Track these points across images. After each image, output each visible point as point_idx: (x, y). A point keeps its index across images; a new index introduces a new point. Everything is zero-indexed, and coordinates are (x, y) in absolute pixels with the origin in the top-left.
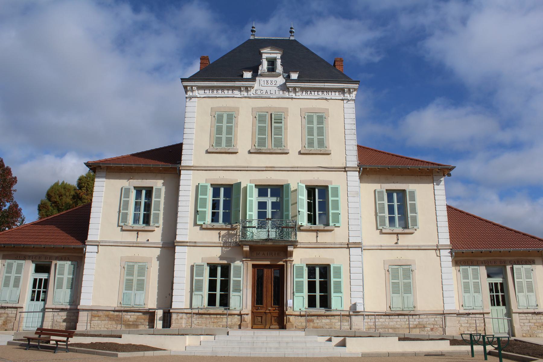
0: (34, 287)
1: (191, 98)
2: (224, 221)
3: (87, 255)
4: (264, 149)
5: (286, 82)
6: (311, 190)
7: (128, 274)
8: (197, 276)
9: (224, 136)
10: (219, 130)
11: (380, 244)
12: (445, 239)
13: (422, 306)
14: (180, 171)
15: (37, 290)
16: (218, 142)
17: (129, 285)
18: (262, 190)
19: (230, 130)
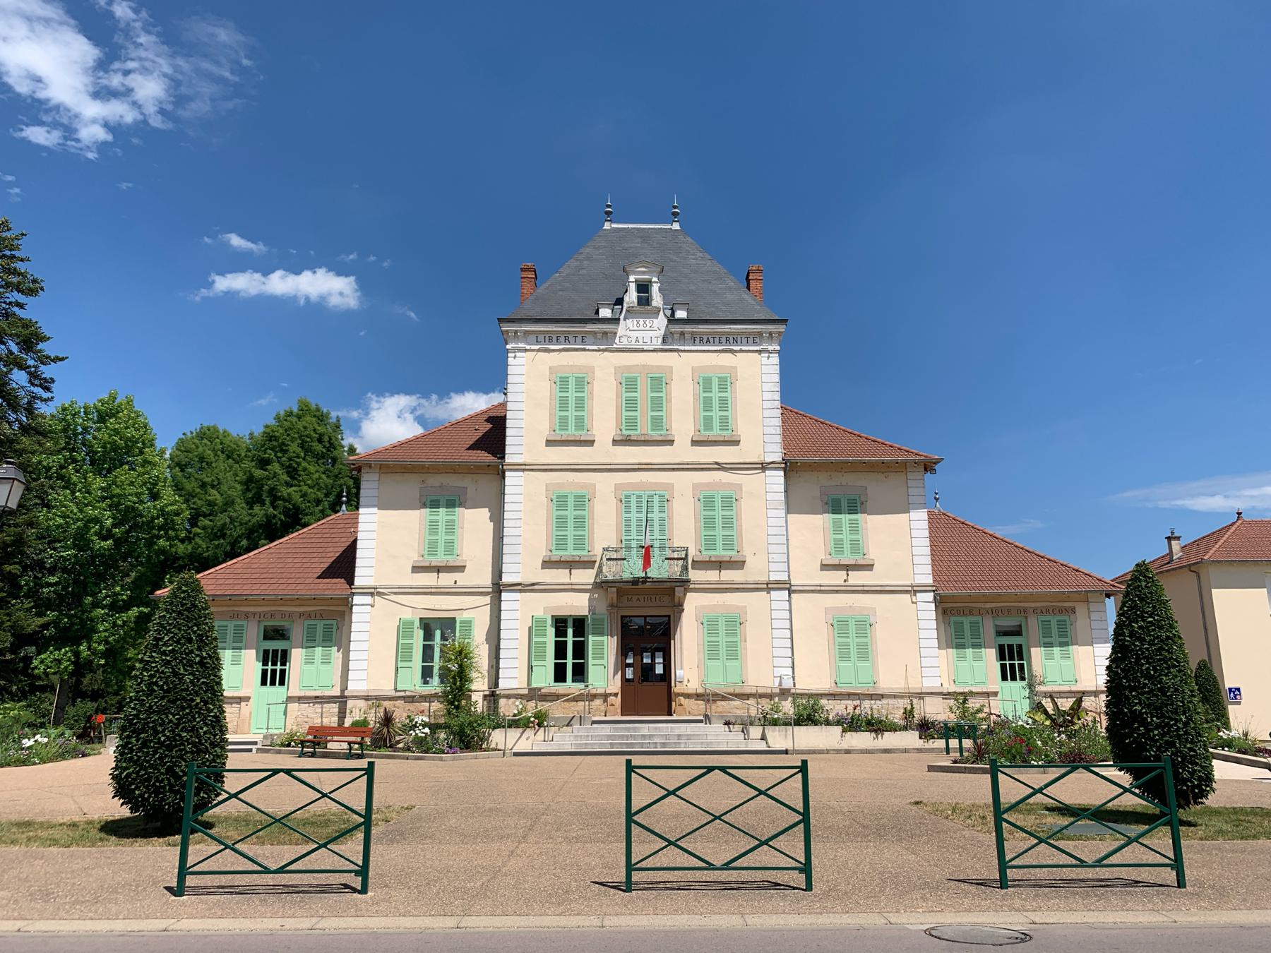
3: (355, 609)
4: (634, 434)
11: (817, 582)
13: (888, 683)
14: (504, 472)
15: (270, 667)
19: (580, 404)
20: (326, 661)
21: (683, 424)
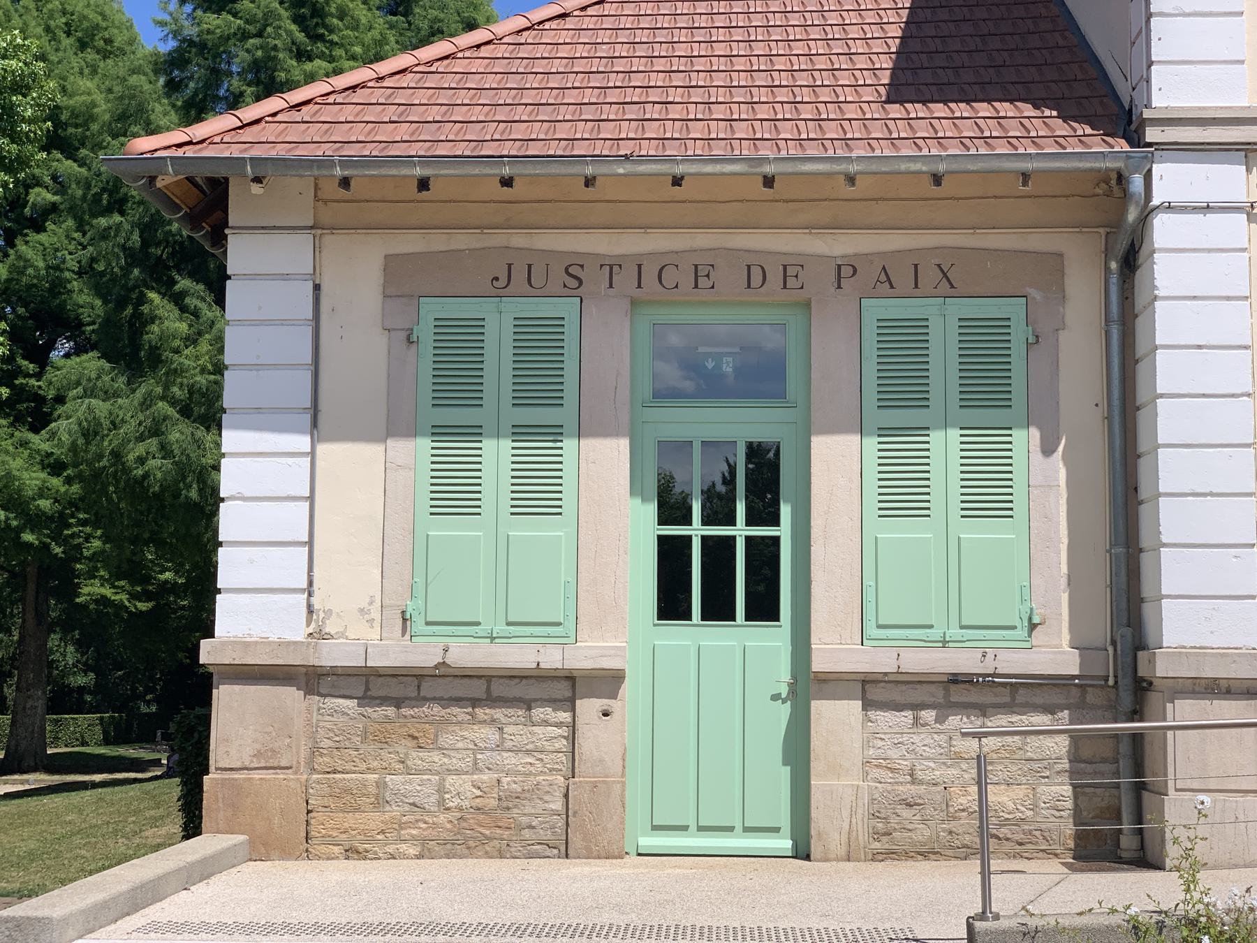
20: (988, 498)
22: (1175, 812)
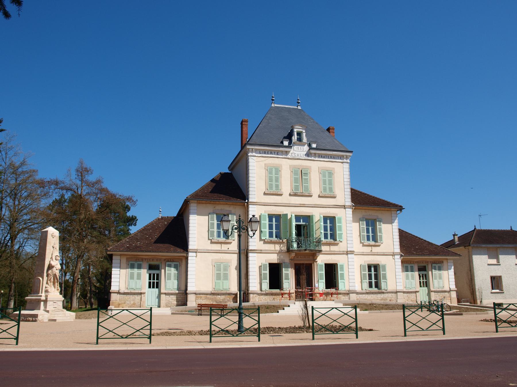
0: (150, 279)
1: (251, 156)
2: (276, 237)
5: (309, 149)
6: (325, 219)
7: (217, 270)
8: (264, 270)
9: (274, 183)
10: (271, 180)
12: (397, 249)
15: (152, 281)
16: (271, 186)
17: (218, 277)
18: (298, 218)
19: (277, 180)
21: (315, 188)
22: (188, 303)
